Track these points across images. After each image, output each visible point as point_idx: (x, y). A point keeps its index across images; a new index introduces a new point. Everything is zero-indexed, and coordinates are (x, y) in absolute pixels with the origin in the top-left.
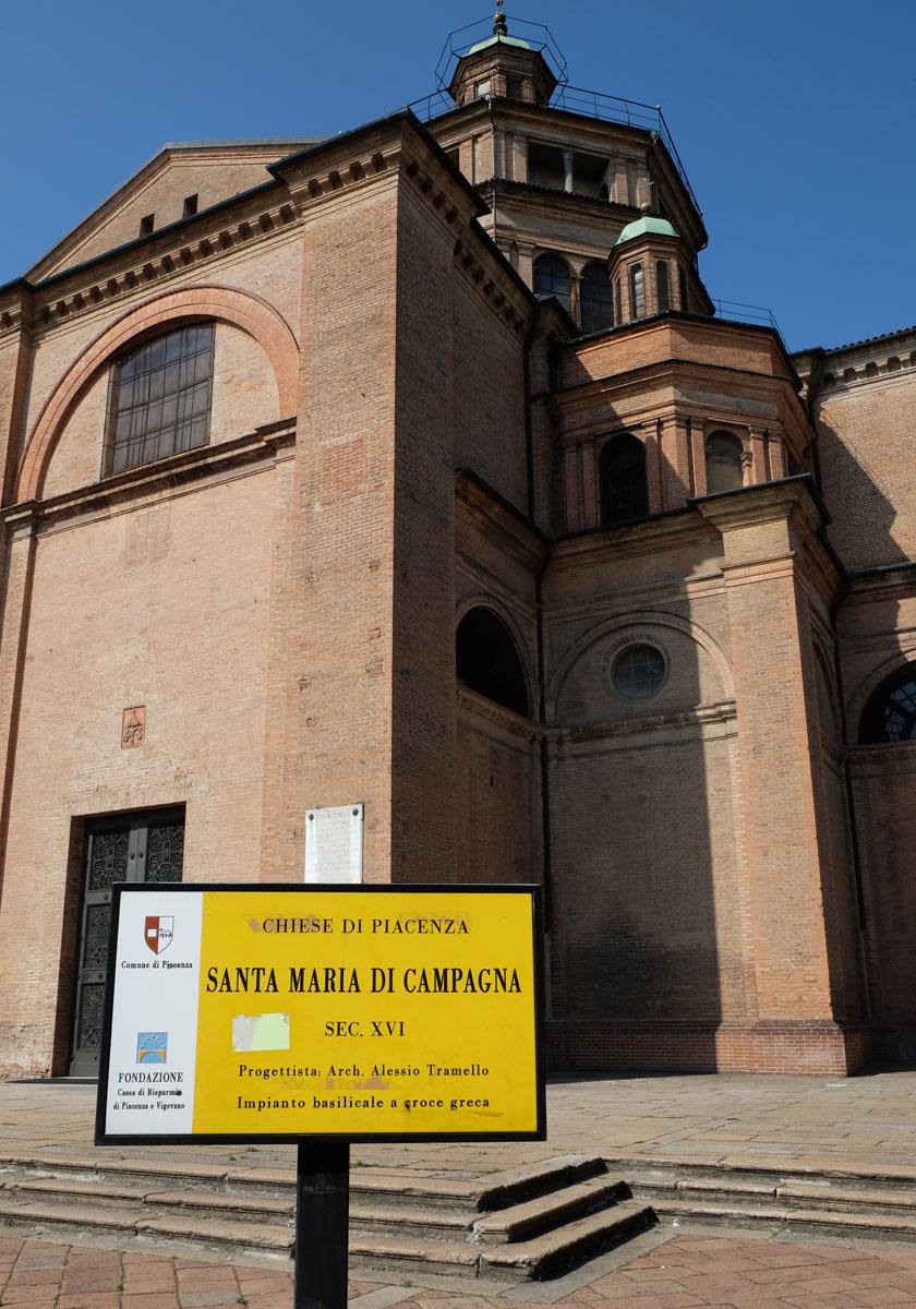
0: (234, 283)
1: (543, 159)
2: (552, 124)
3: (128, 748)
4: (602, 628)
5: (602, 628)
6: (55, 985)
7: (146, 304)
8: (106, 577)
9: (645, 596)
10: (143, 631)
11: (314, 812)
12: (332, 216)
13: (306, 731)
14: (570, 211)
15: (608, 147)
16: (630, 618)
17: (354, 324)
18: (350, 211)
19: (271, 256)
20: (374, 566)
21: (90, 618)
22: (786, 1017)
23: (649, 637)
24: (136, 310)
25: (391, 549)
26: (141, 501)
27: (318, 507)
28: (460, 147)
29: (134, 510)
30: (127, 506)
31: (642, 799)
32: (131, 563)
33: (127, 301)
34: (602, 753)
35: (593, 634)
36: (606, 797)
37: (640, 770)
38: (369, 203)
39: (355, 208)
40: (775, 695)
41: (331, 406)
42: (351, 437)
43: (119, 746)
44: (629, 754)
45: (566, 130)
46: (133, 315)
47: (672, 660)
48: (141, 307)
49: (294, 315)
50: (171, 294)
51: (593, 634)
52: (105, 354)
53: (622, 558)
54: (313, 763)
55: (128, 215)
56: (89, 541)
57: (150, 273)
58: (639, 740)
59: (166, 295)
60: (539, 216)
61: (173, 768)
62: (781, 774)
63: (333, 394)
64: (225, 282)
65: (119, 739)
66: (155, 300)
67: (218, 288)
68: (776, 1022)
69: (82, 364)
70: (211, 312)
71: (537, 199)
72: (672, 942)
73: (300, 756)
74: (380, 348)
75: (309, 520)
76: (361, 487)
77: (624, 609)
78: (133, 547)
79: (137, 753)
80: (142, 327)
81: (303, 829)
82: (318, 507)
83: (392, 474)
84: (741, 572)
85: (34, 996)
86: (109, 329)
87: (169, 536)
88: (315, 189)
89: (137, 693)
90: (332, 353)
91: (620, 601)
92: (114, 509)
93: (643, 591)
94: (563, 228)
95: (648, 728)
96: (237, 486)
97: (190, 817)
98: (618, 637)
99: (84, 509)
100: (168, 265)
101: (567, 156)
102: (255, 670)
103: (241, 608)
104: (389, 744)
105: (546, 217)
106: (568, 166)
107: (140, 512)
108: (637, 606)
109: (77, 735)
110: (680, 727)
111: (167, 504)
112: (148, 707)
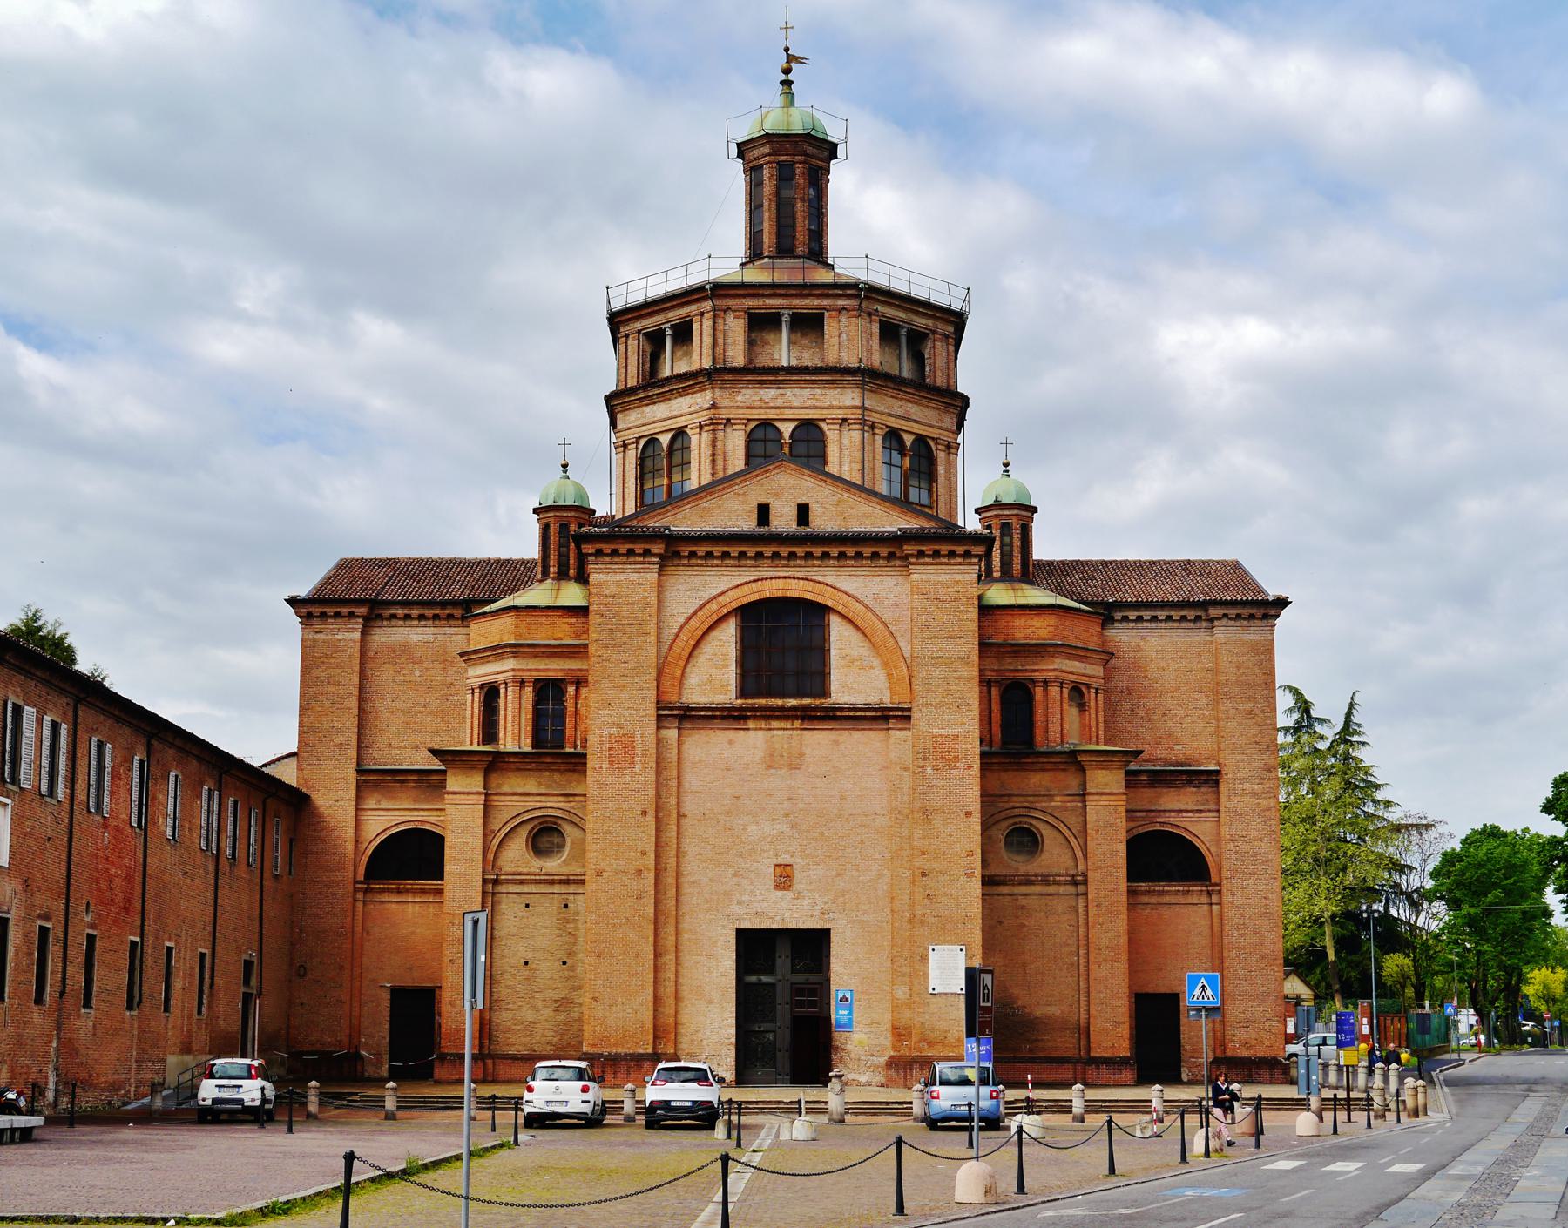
0: (847, 589)
1: (889, 333)
2: (898, 306)
3: (781, 889)
4: (1003, 815)
5: (1003, 815)
6: (733, 1031)
7: (771, 578)
8: (749, 772)
9: (1031, 799)
10: (787, 815)
11: (935, 947)
12: (931, 576)
13: (927, 902)
14: (909, 393)
15: (930, 323)
16: (1023, 812)
17: (950, 658)
18: (944, 578)
19: (878, 579)
20: (969, 814)
21: (738, 798)
22: (1106, 1055)
23: (1031, 825)
24: (762, 579)
25: (979, 806)
26: (775, 724)
27: (929, 770)
28: (826, 314)
29: (770, 729)
30: (762, 724)
31: (1023, 926)
32: (770, 767)
33: (752, 569)
34: (998, 895)
35: (997, 817)
36: (1000, 922)
37: (1023, 907)
38: (959, 577)
39: (949, 576)
40: (1111, 875)
41: (935, 707)
42: (950, 732)
43: (772, 887)
44: (1015, 897)
45: (905, 309)
46: (760, 582)
47: (1046, 842)
48: (766, 579)
49: (900, 629)
50: (794, 578)
51: (997, 817)
52: (734, 605)
53: (1017, 770)
54: (932, 920)
55: (744, 494)
56: (731, 742)
57: (776, 556)
58: (1023, 889)
59: (790, 578)
60: (887, 395)
61: (819, 907)
62: (1111, 922)
63: (938, 700)
64: (838, 586)
65: (772, 883)
66: (779, 578)
67: (834, 588)
68: (1100, 1058)
69: (713, 606)
70: (829, 603)
71: (890, 384)
72: (1038, 1012)
73: (924, 915)
74: (969, 679)
75: (923, 777)
76: (958, 765)
77: (1018, 805)
78: (772, 755)
79: (789, 895)
80: (768, 595)
81: (927, 955)
82: (929, 770)
83: (979, 762)
84: (1096, 797)
85: (715, 1038)
86: (738, 586)
87: (802, 755)
88: (921, 554)
89: (783, 856)
90: (938, 673)
91: (1015, 799)
92: (751, 724)
93: (1030, 796)
94: (901, 406)
95: (1029, 882)
96: (857, 735)
97: (835, 940)
98: (1011, 821)
99: (723, 718)
100: (792, 556)
101: (904, 332)
102: (877, 856)
103: (866, 816)
104: (980, 916)
105: (892, 397)
106: (904, 340)
107: (775, 732)
108: (1026, 804)
109: (735, 875)
110: (1049, 885)
111: (799, 732)
112: (794, 866)
